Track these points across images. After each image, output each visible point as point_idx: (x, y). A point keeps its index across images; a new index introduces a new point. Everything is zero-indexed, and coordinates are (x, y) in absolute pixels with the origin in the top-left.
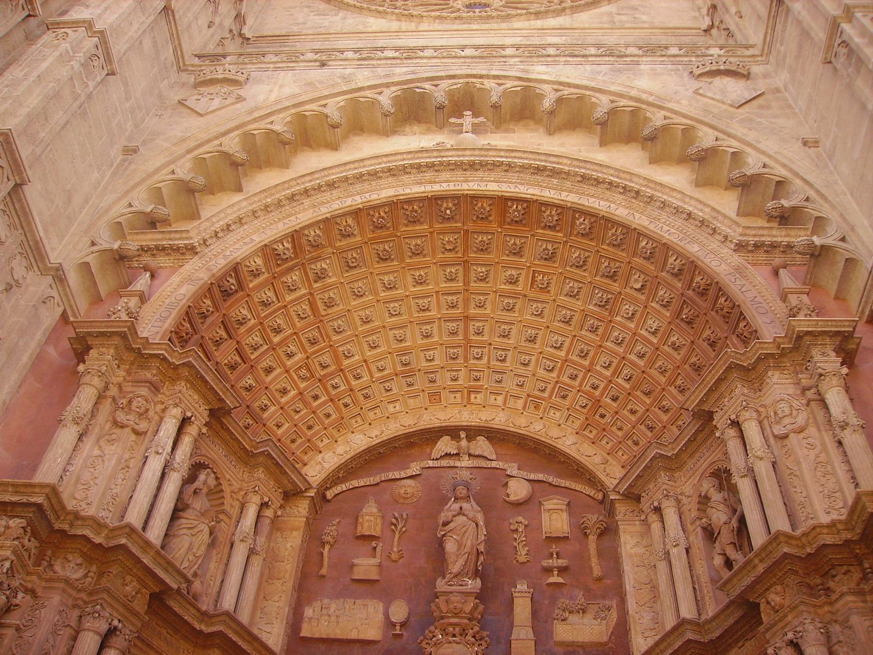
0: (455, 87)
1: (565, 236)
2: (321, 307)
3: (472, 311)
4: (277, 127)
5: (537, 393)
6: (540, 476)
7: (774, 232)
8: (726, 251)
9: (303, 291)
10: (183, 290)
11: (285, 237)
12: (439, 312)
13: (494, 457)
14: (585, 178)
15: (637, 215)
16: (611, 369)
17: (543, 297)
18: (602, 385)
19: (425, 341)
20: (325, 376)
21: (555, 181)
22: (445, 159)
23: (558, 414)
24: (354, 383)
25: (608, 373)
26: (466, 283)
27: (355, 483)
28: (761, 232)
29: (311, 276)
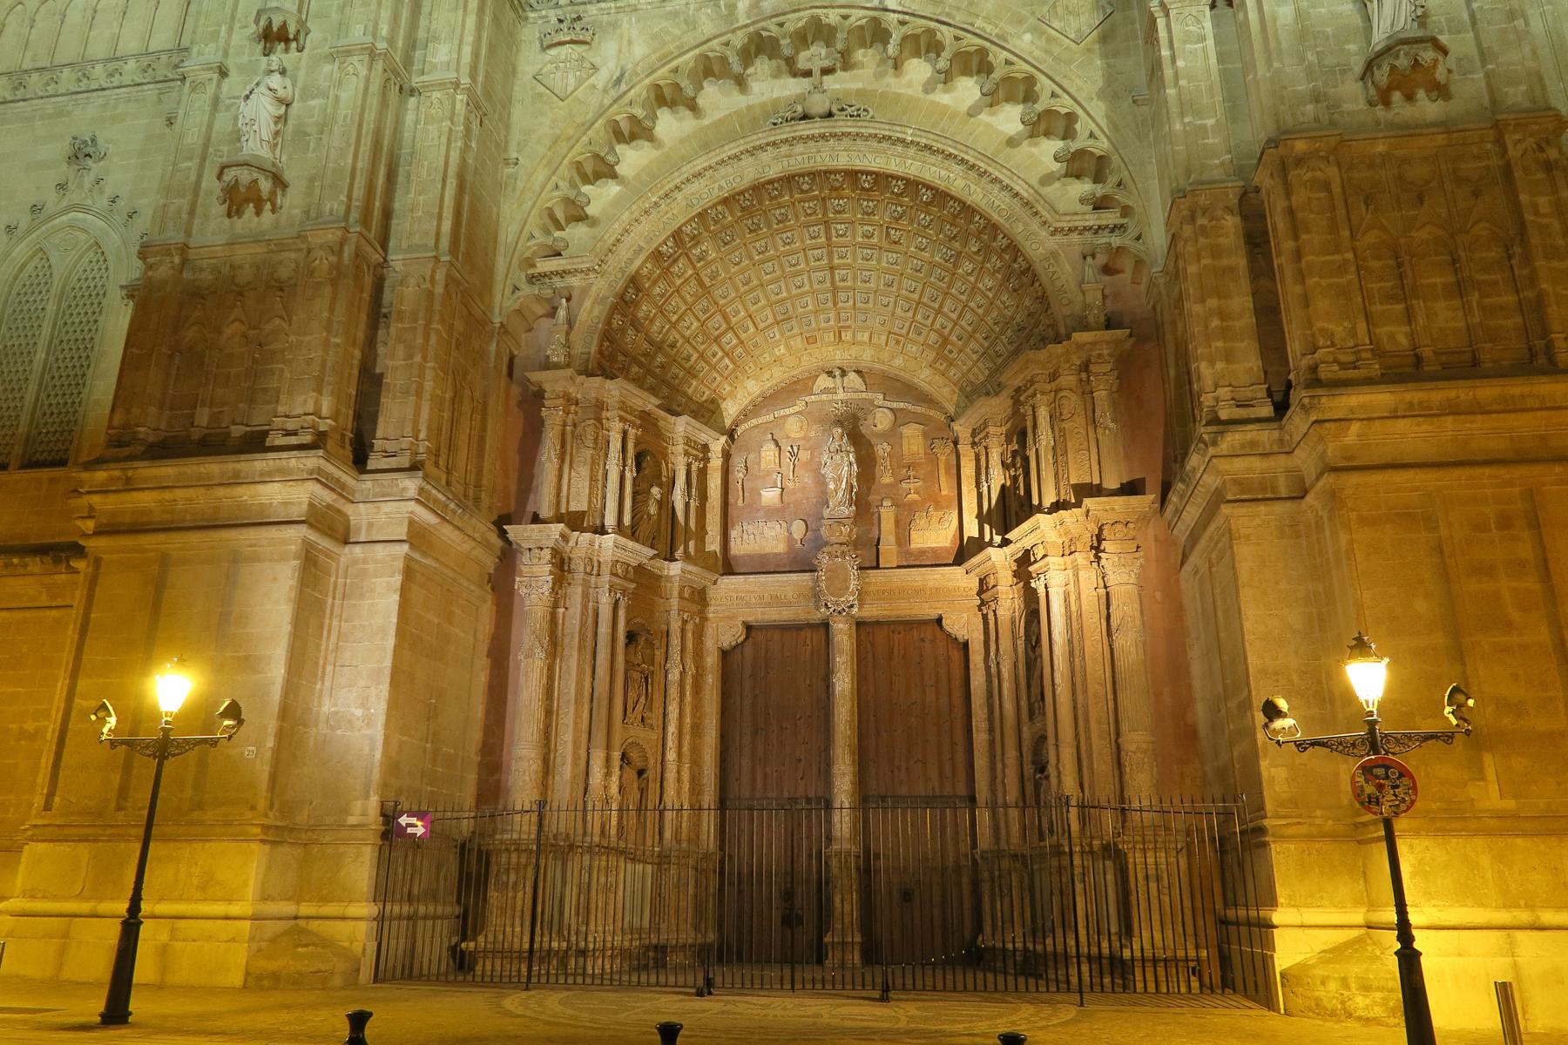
0: (800, 24)
1: (911, 200)
2: (707, 281)
3: (836, 261)
4: (639, 112)
5: (896, 330)
6: (901, 405)
7: (1087, 217)
8: (1044, 233)
9: (690, 272)
10: (596, 313)
11: (668, 238)
12: (807, 263)
13: (864, 388)
14: (928, 148)
15: (973, 187)
16: (957, 313)
17: (896, 247)
18: (950, 326)
19: (798, 291)
20: (719, 336)
21: (899, 148)
22: (797, 134)
23: (914, 348)
24: (743, 336)
25: (954, 316)
26: (829, 238)
27: (754, 422)
28: (1075, 217)
29: (694, 259)
